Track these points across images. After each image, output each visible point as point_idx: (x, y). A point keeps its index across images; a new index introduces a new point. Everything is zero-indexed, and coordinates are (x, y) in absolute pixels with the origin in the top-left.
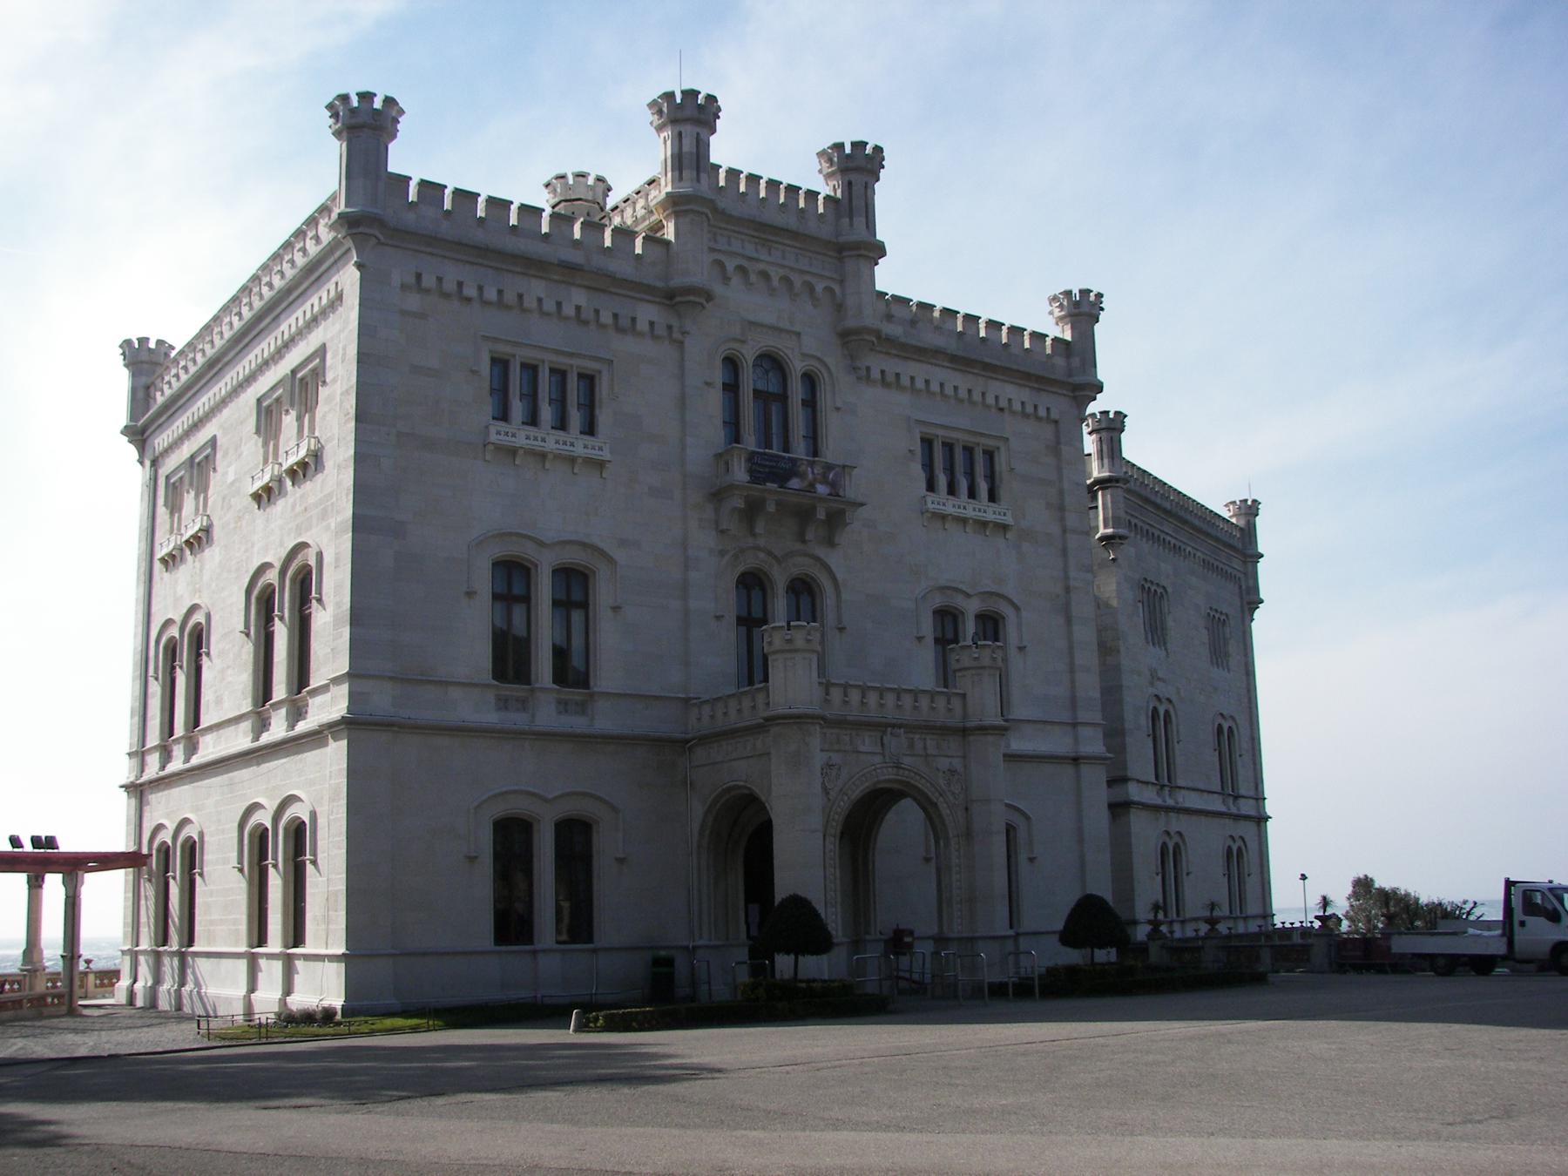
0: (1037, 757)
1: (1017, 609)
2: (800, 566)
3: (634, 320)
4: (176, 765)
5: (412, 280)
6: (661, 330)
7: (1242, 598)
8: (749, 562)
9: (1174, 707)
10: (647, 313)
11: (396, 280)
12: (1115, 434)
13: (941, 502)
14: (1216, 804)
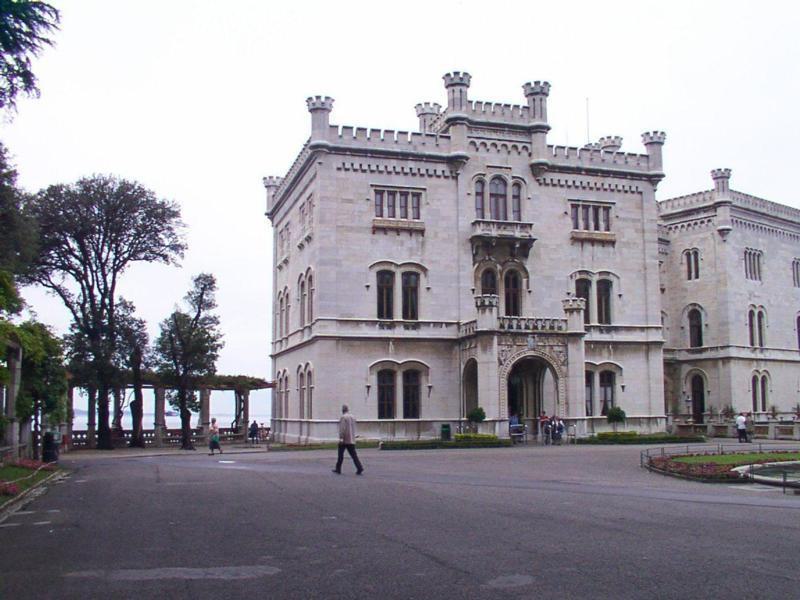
1: (618, 278)
2: (510, 266)
3: (435, 171)
4: (283, 349)
5: (340, 165)
6: (447, 173)
8: (489, 265)
10: (441, 168)
11: (335, 168)
12: (725, 181)
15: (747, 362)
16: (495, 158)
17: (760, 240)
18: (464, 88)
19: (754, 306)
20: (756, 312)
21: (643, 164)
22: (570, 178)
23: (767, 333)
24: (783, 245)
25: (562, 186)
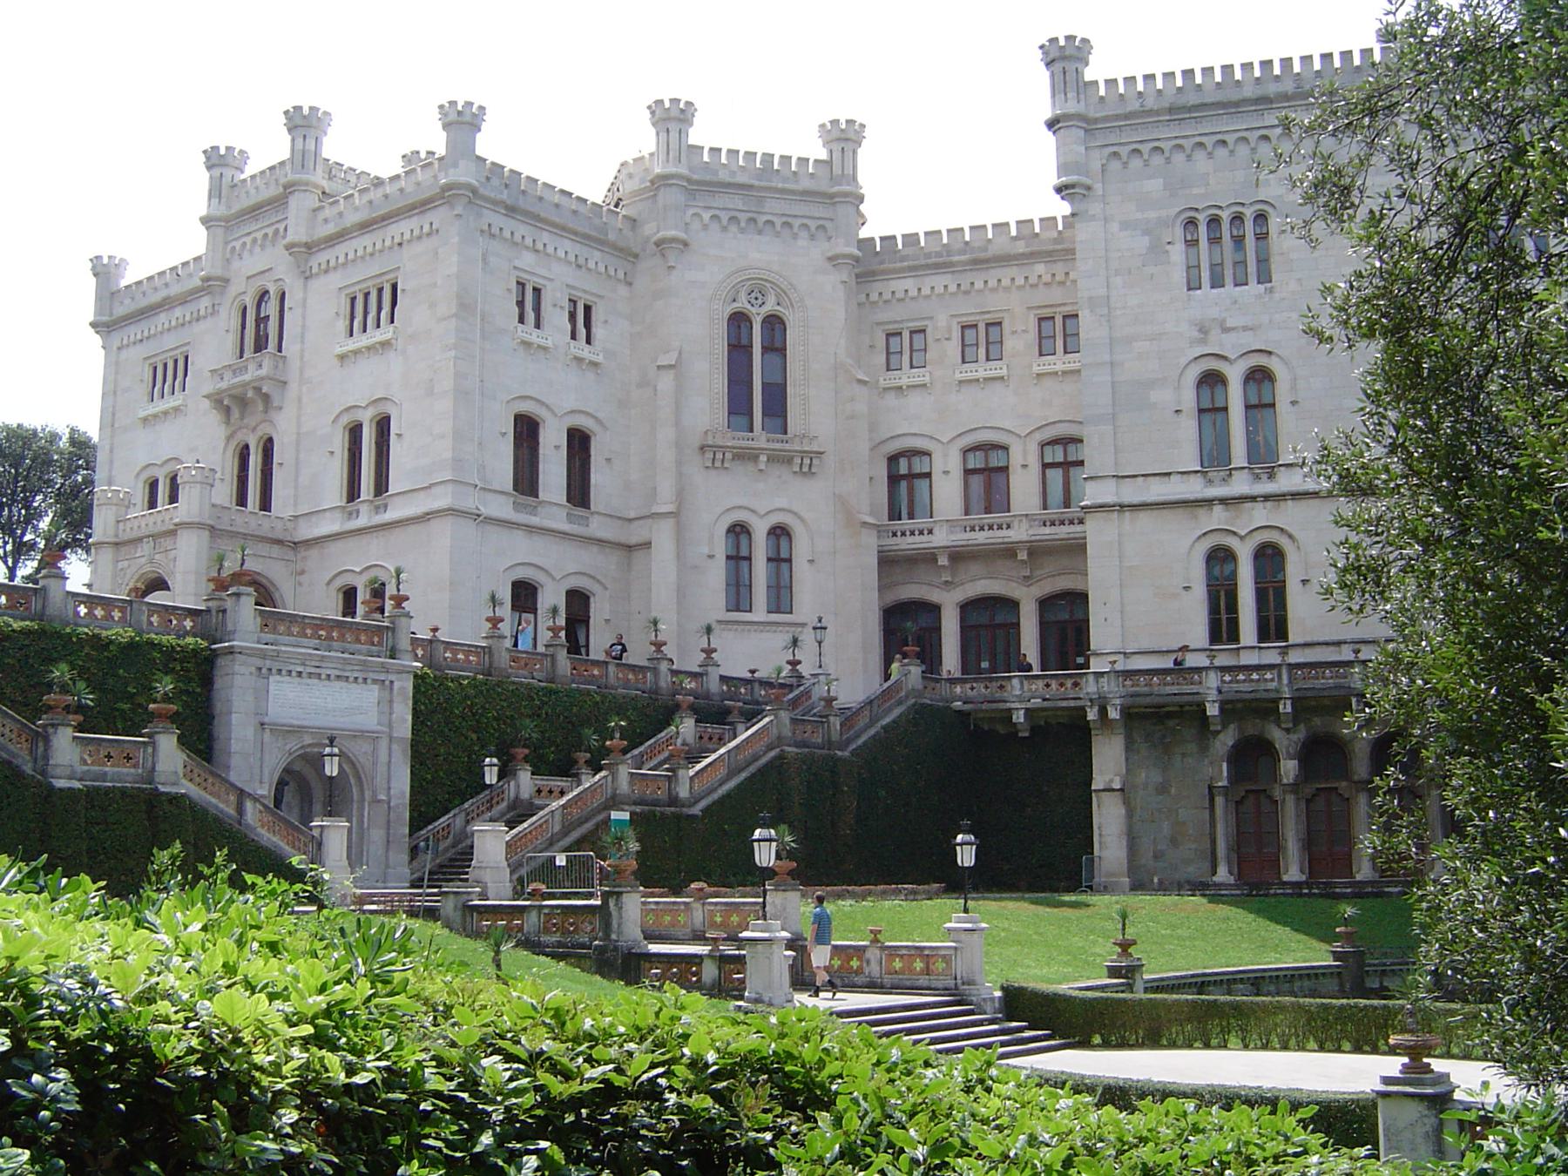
2: (265, 430)
9: (1278, 356)
10: (204, 303)
12: (1058, 66)
13: (361, 341)
15: (1180, 513)
16: (253, 262)
20: (1235, 375)
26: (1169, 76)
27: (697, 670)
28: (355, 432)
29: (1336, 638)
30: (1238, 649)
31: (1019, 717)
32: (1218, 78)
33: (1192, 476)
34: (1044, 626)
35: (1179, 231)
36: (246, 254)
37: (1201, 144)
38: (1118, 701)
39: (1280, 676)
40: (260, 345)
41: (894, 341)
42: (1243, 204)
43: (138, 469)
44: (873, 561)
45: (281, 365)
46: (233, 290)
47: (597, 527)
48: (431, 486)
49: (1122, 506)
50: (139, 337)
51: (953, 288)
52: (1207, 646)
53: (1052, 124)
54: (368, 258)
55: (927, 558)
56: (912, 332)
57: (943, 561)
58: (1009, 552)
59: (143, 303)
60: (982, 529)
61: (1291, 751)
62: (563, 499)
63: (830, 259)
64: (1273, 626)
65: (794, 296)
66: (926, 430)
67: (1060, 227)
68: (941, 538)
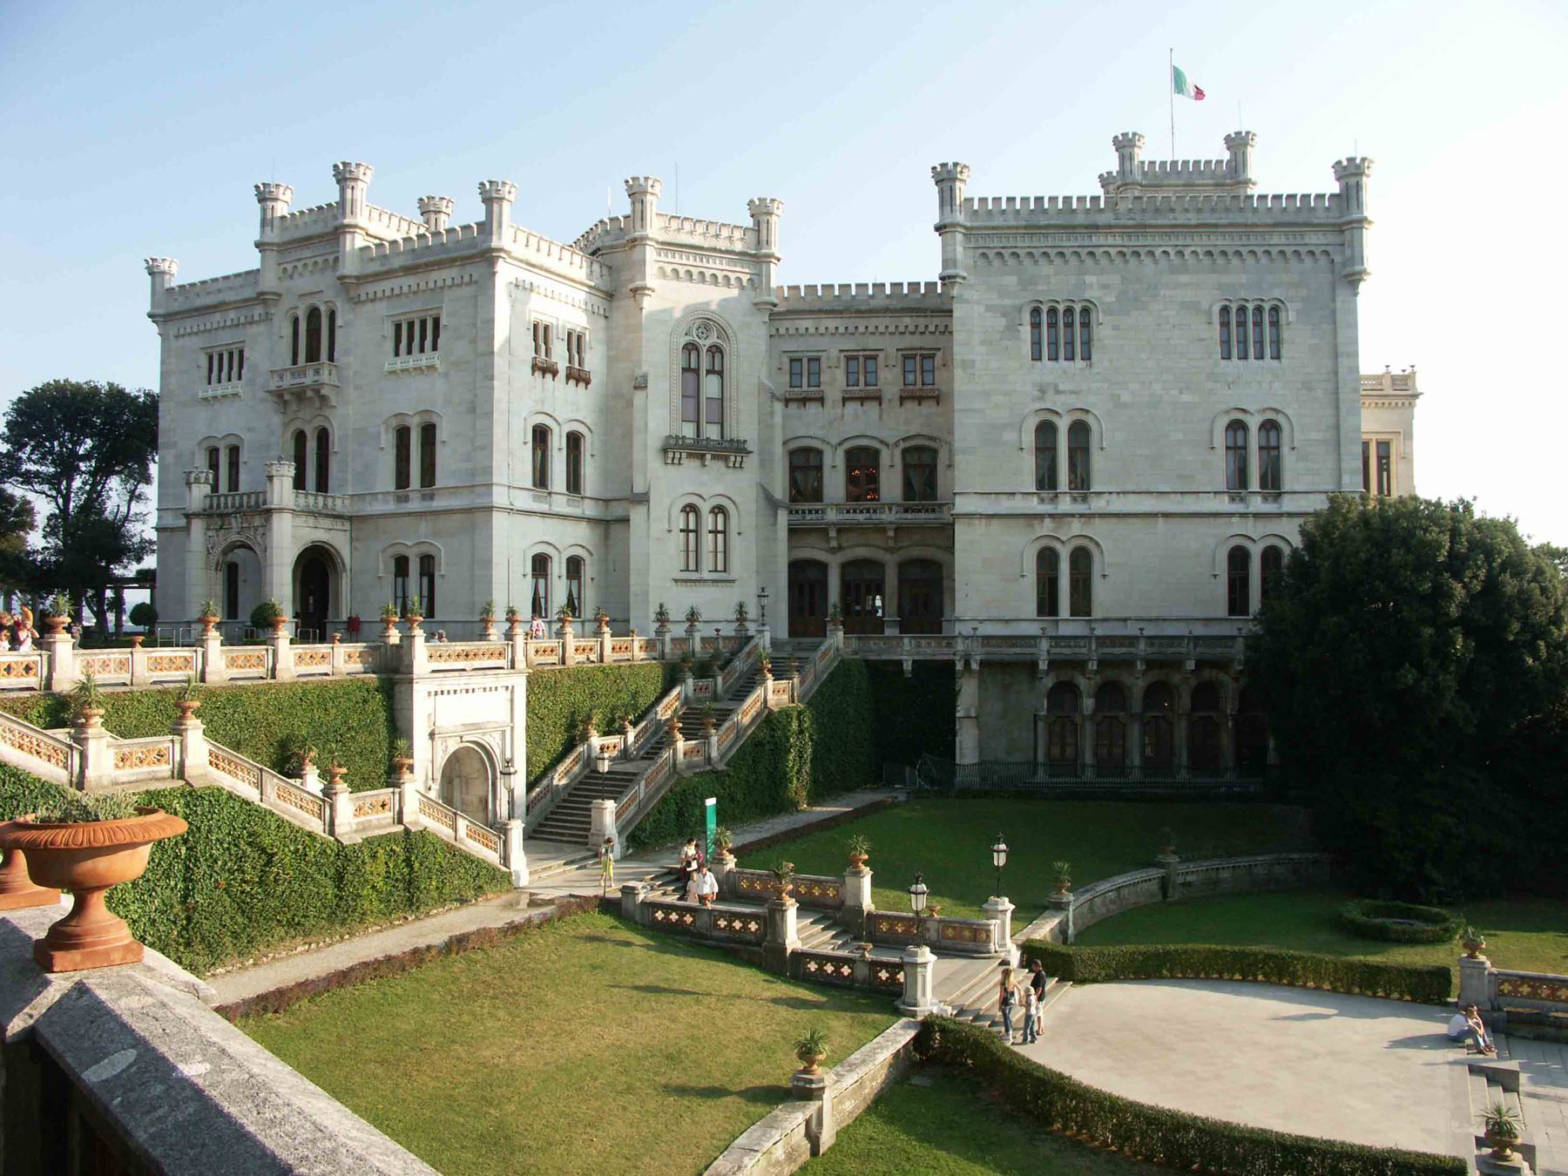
0: (452, 510)
2: (319, 422)
7: (1333, 272)
10: (258, 311)
12: (946, 185)
14: (1223, 504)
15: (1022, 521)
16: (305, 283)
17: (1091, 279)
18: (270, 204)
19: (1057, 413)
20: (1063, 425)
21: (482, 238)
22: (385, 286)
23: (1098, 461)
24: (1183, 278)
25: (381, 299)
26: (1025, 200)
27: (683, 634)
28: (403, 434)
29: (1124, 615)
30: (1057, 621)
31: (908, 666)
32: (1060, 206)
33: (1030, 497)
34: (901, 581)
35: (1027, 318)
36: (296, 276)
37: (1045, 254)
38: (978, 658)
39: (1090, 643)
40: (313, 355)
41: (796, 365)
42: (1073, 301)
43: (200, 438)
44: (783, 533)
45: (334, 372)
46: (286, 303)
47: (589, 509)
48: (473, 486)
49: (981, 515)
50: (195, 330)
51: (842, 330)
52: (1036, 618)
53: (938, 229)
54: (411, 295)
55: (822, 531)
56: (809, 360)
57: (833, 534)
58: (880, 529)
59: (198, 303)
60: (861, 512)
61: (1091, 691)
62: (564, 489)
63: (755, 304)
64: (1082, 605)
65: (729, 332)
66: (820, 433)
67: (923, 291)
68: (832, 516)
